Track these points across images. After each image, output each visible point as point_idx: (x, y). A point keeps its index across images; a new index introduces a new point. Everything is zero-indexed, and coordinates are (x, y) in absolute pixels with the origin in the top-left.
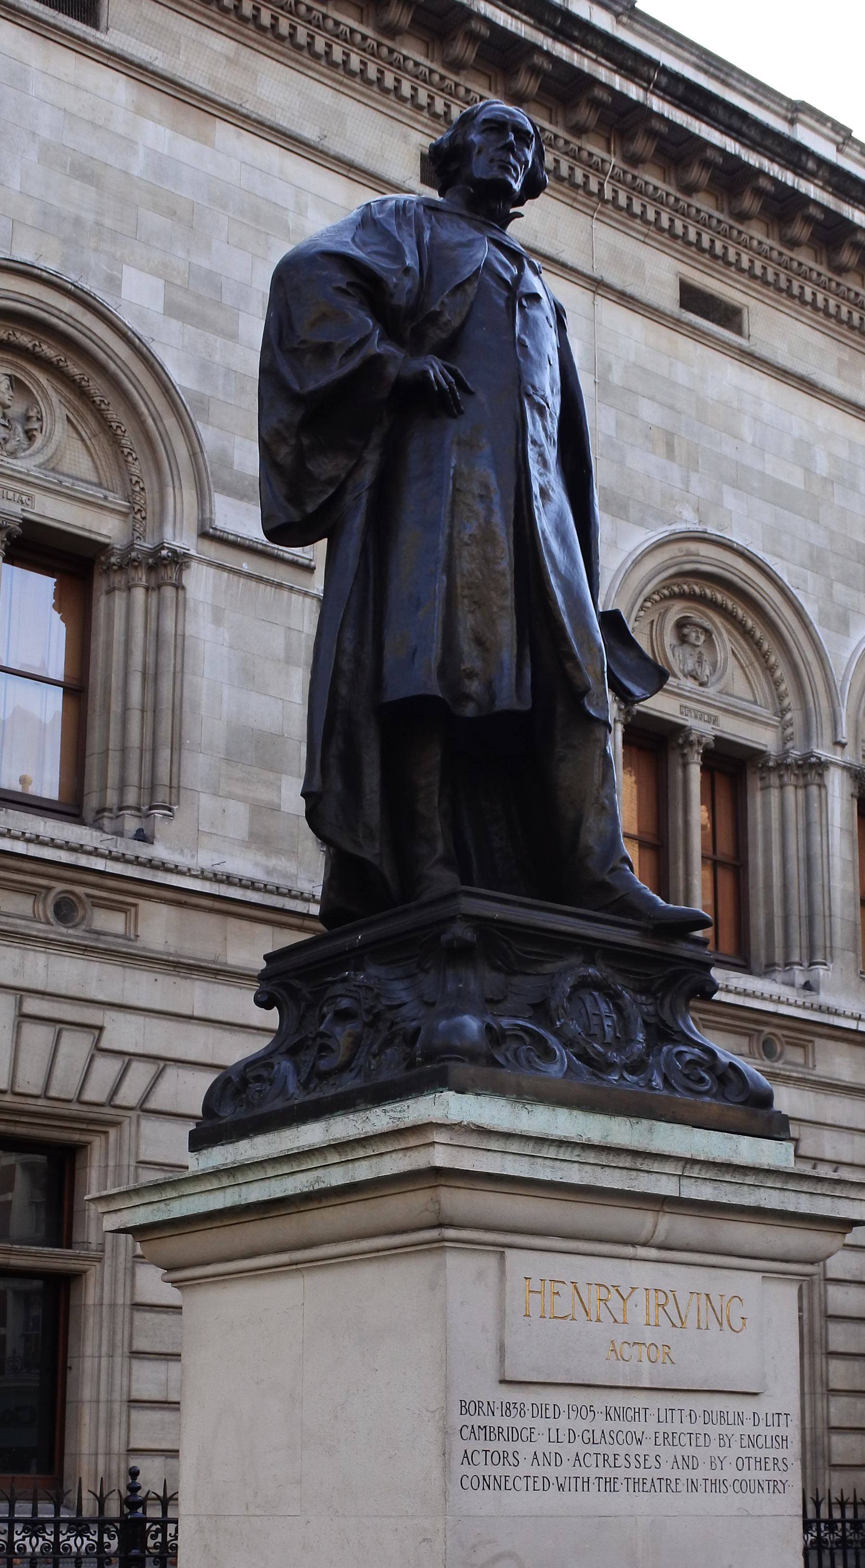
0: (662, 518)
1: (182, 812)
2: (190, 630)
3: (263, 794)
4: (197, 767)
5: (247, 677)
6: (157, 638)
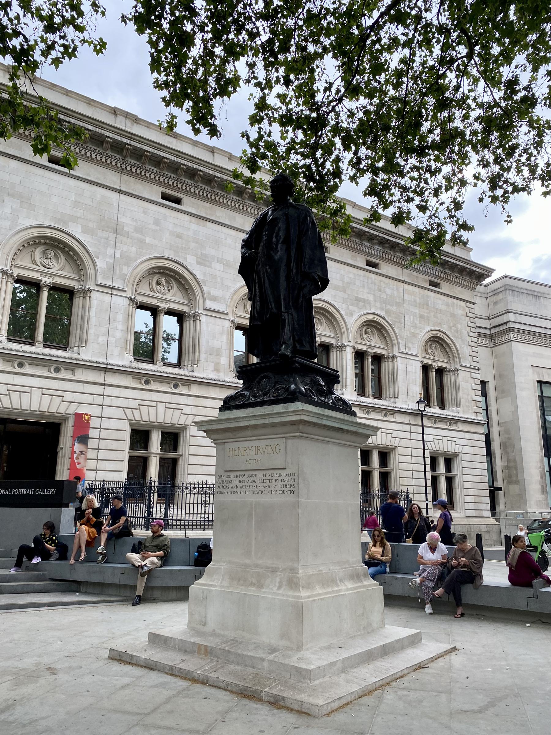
4: (203, 356)
6: (195, 330)
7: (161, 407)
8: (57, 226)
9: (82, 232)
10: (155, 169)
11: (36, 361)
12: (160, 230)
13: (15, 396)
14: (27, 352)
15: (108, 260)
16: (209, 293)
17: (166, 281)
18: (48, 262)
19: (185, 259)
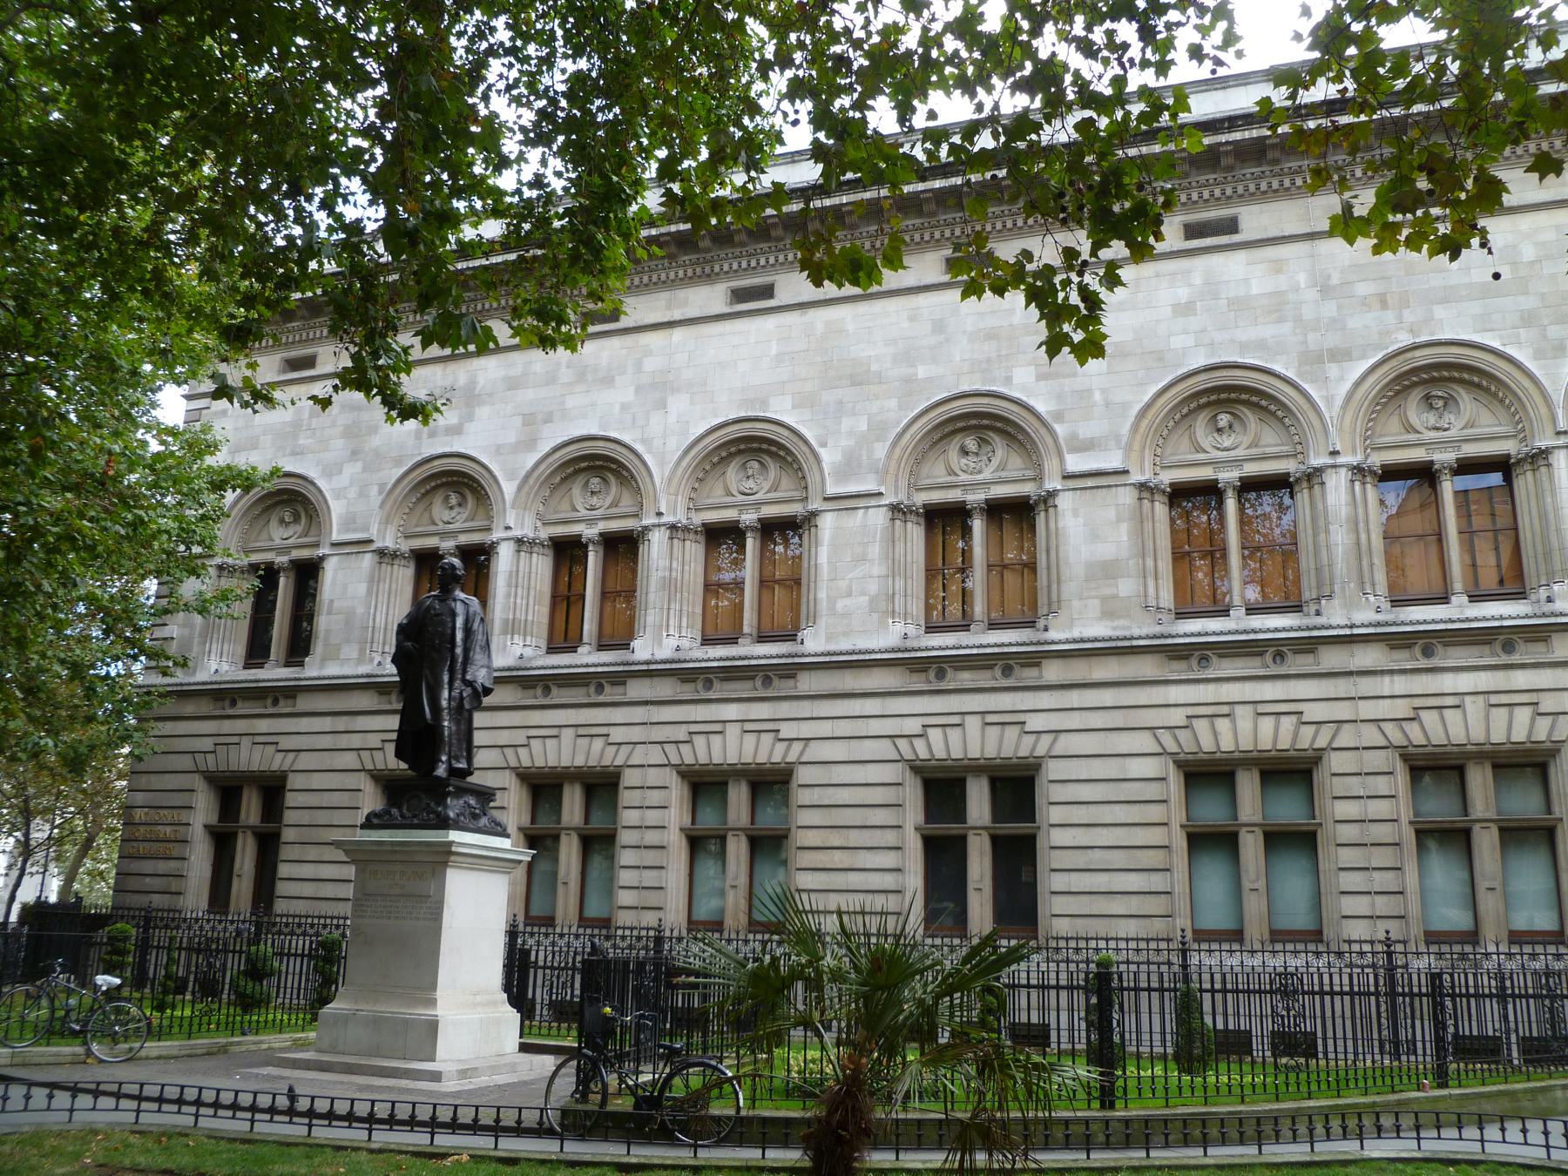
0: (1378, 348)
1: (1063, 613)
2: (1061, 525)
3: (1108, 591)
4: (1069, 589)
5: (1094, 536)
7: (973, 723)
8: (750, 414)
9: (794, 407)
10: (917, 221)
11: (731, 673)
12: (947, 340)
13: (700, 741)
14: (709, 660)
15: (844, 443)
16: (1073, 437)
17: (982, 442)
18: (751, 484)
19: (1008, 380)
